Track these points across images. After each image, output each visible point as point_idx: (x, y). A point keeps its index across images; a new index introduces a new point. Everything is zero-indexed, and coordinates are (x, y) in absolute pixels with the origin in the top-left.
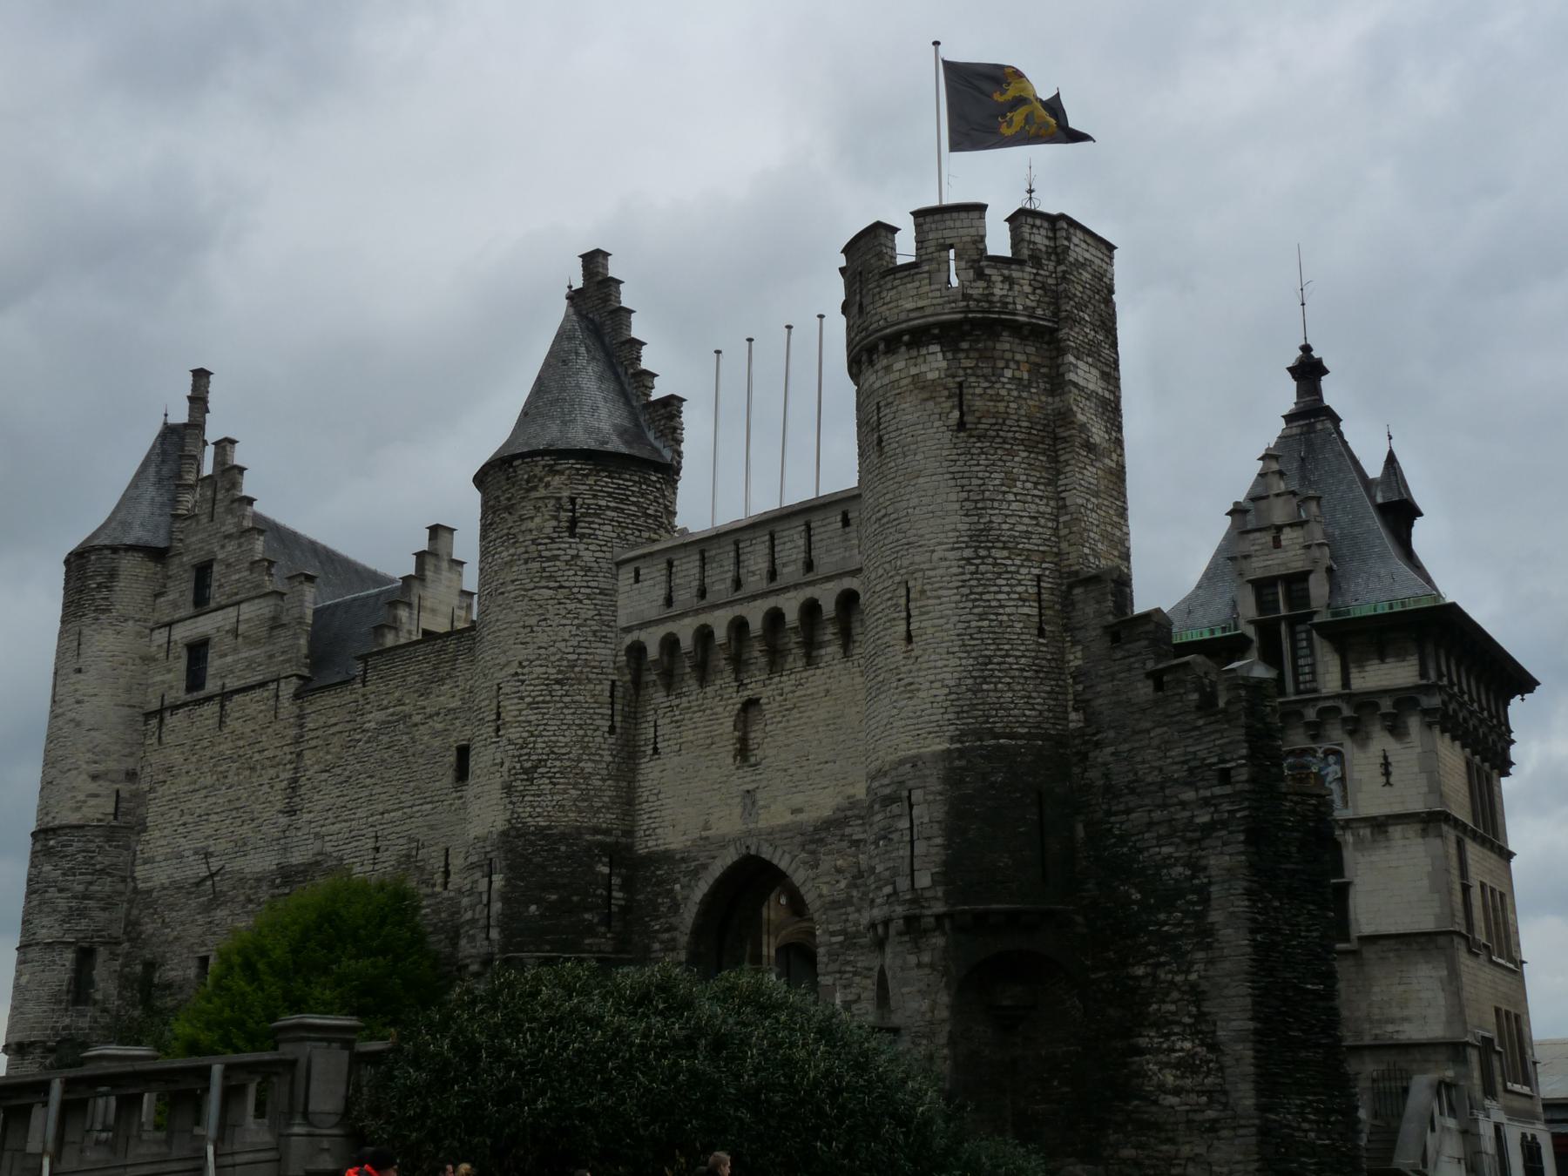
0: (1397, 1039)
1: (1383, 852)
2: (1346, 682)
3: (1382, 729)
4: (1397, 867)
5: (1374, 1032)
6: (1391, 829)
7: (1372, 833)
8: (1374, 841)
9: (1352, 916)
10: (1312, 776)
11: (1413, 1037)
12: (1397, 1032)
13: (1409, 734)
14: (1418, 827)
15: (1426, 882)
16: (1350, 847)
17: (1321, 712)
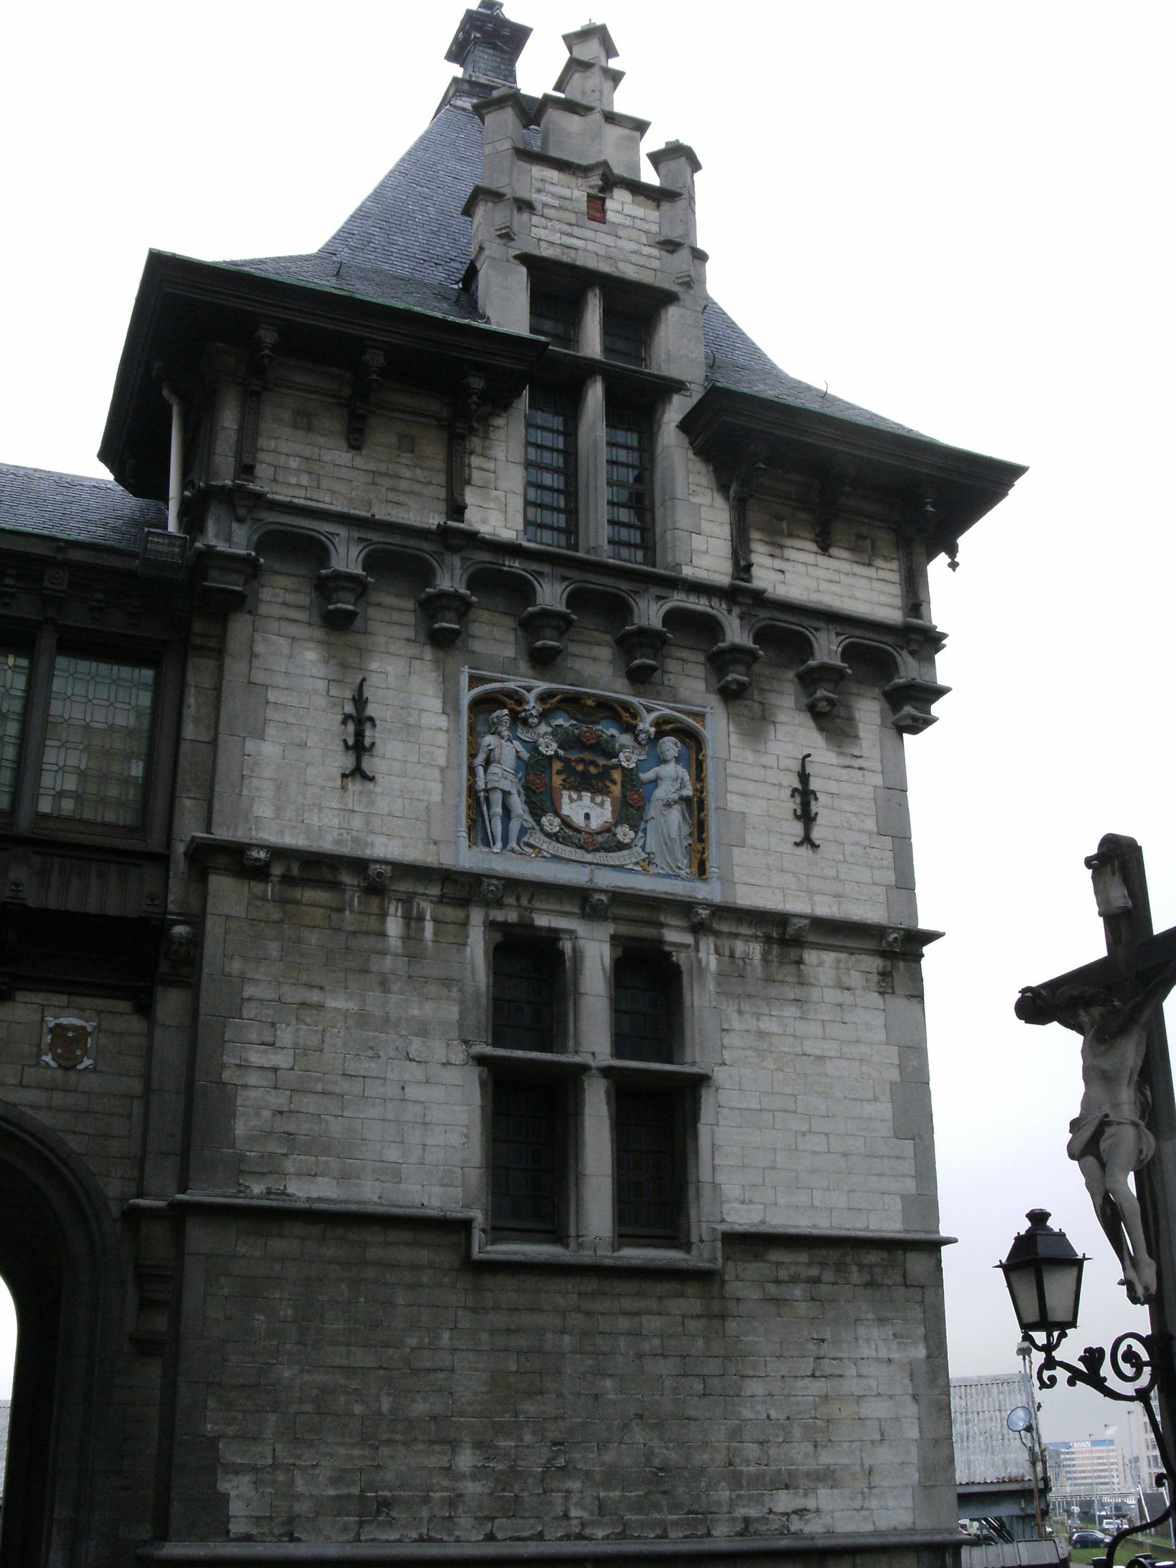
0: (799, 1534)
1: (790, 1011)
2: (743, 569)
3: (798, 709)
4: (820, 1058)
5: (741, 1512)
6: (811, 957)
7: (765, 959)
8: (769, 980)
9: (705, 1175)
10: (617, 775)
11: (839, 1529)
12: (801, 1512)
13: (856, 737)
14: (874, 963)
15: (884, 1109)
16: (711, 986)
17: (674, 618)
